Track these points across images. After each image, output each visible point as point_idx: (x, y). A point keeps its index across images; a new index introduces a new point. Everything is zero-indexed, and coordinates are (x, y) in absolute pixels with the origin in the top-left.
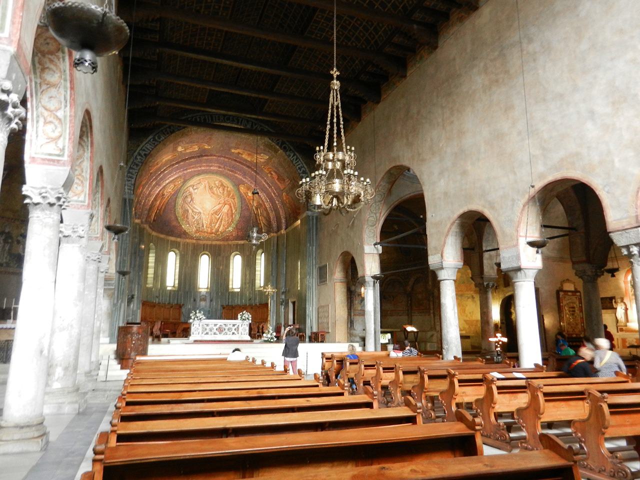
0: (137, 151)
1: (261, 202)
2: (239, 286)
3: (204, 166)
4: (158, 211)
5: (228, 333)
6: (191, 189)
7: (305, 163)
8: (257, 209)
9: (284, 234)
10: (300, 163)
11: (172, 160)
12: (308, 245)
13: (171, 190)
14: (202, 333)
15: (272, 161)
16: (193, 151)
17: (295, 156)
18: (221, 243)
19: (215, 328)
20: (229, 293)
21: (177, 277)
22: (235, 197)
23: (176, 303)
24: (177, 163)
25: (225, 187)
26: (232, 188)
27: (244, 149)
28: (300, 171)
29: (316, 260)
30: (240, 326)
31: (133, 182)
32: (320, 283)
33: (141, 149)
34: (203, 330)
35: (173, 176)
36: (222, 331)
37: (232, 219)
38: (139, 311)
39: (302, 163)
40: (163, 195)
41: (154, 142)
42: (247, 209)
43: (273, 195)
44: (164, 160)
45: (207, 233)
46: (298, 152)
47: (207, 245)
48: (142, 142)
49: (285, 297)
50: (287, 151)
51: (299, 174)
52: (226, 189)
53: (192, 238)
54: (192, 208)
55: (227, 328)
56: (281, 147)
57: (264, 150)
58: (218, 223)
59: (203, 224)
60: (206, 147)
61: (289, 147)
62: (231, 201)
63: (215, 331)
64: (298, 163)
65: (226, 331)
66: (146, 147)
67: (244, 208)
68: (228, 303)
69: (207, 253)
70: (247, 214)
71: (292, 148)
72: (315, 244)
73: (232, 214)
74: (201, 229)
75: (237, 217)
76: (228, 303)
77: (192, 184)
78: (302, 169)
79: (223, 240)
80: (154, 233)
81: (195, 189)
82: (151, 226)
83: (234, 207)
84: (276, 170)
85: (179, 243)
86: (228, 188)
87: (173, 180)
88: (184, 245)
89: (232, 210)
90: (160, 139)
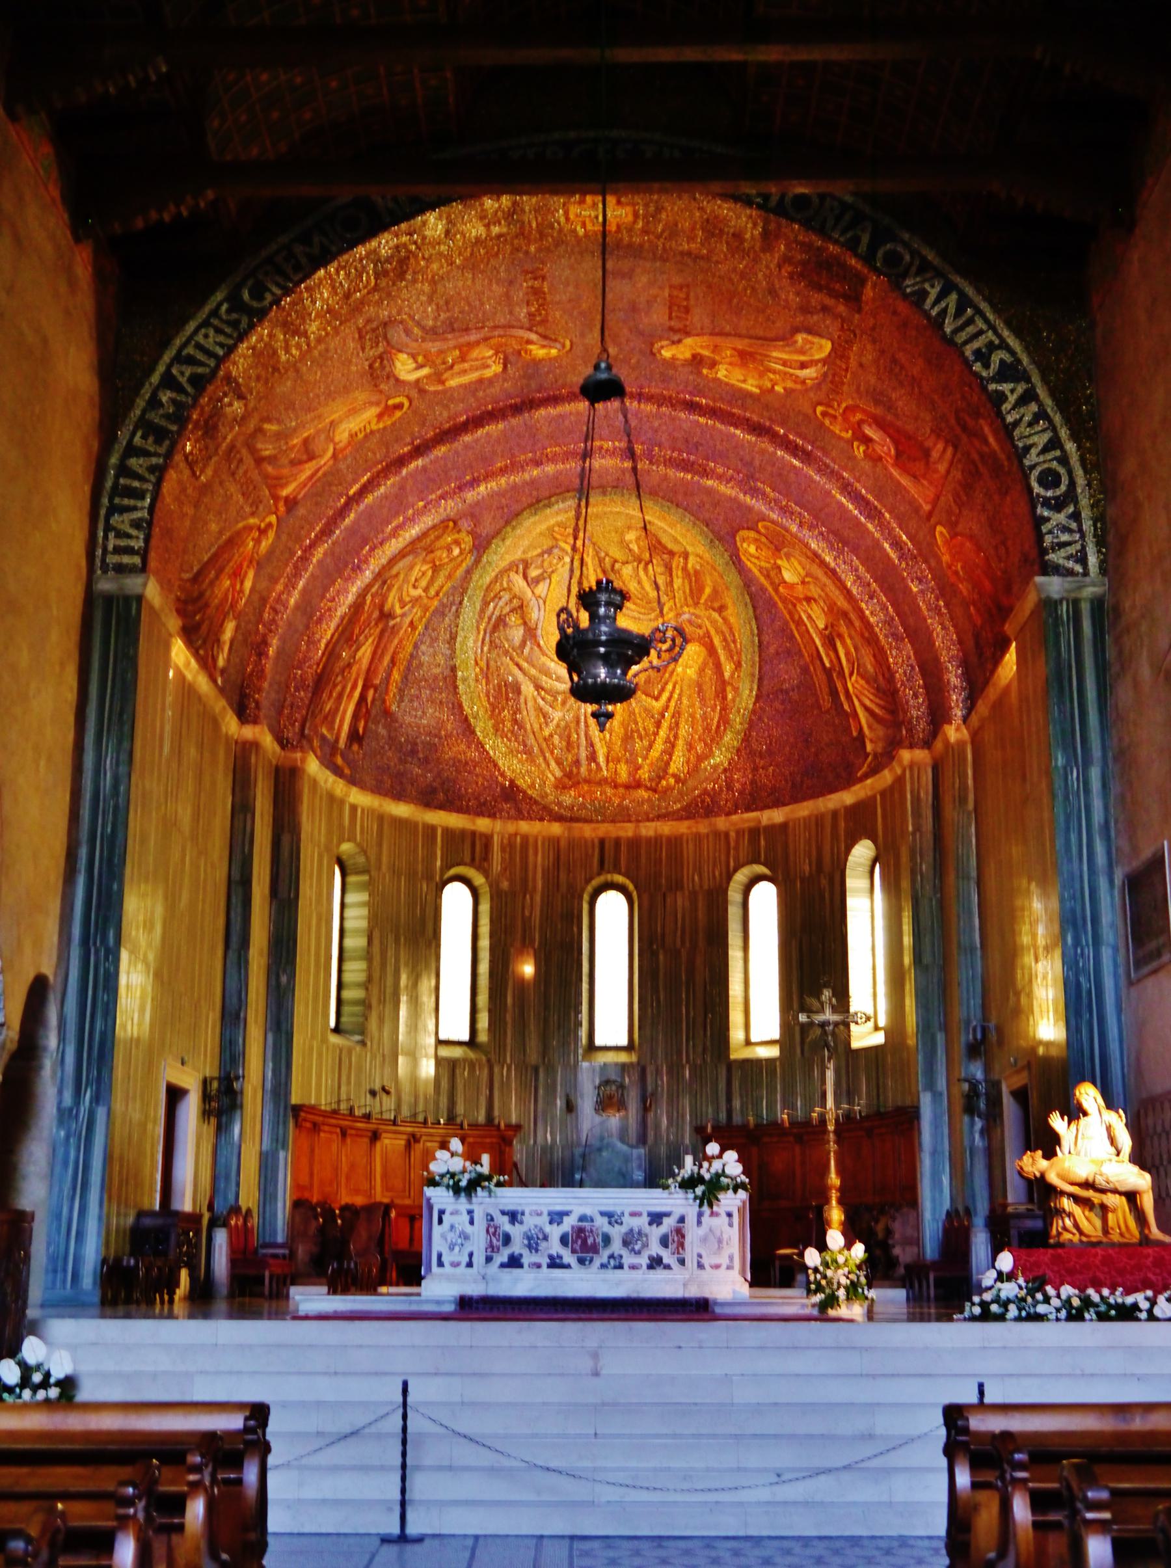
0: (161, 368)
1: (842, 603)
2: (776, 1034)
3: (553, 459)
4: (371, 694)
5: (627, 1259)
6: (518, 581)
7: (1008, 324)
8: (830, 643)
9: (961, 744)
10: (981, 324)
11: (386, 437)
12: (1060, 761)
13: (419, 592)
14: (489, 1259)
15: (853, 363)
16: (480, 381)
17: (954, 297)
18: (683, 828)
19: (555, 1232)
20: (731, 1065)
21: (483, 999)
22: (729, 602)
23: (481, 1118)
24: (418, 451)
25: (672, 554)
26: (707, 556)
27: (712, 334)
28: (987, 366)
29: (1107, 839)
30: (691, 1219)
31: (145, 514)
32: (1138, 965)
33: (179, 359)
34: (491, 1247)
35: (412, 520)
36: (594, 1249)
37: (723, 709)
38: (282, 1154)
39: (992, 327)
40: (386, 616)
41: (234, 316)
42: (788, 652)
43: (893, 555)
44: (342, 435)
45: (616, 787)
46: (975, 278)
47: (617, 841)
48: (184, 321)
49: (987, 1069)
50: (905, 276)
51: (982, 383)
52: (678, 562)
53: (547, 813)
54: (533, 671)
55: (616, 1233)
56: (868, 259)
57: (805, 309)
58: (663, 733)
59: (591, 745)
60: (538, 352)
61: (914, 253)
62: (708, 619)
63: (555, 1248)
64: (971, 330)
65: (616, 1247)
66: (199, 346)
67: (772, 650)
68: (730, 1112)
69: (619, 879)
70: (789, 674)
71: (930, 256)
72: (1096, 752)
73: (722, 686)
74: (583, 770)
75: (745, 696)
76: (730, 1112)
77: (518, 555)
78: (997, 357)
79: (689, 813)
80: (358, 797)
81: (537, 581)
82: (339, 760)
83: (727, 647)
84: (879, 411)
85: (487, 839)
86: (686, 555)
87: (419, 539)
88: (509, 846)
89: (718, 667)
90: (261, 298)
